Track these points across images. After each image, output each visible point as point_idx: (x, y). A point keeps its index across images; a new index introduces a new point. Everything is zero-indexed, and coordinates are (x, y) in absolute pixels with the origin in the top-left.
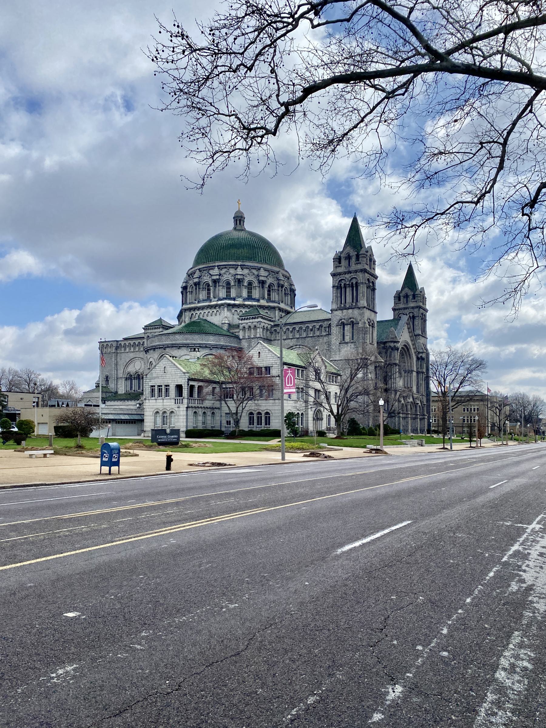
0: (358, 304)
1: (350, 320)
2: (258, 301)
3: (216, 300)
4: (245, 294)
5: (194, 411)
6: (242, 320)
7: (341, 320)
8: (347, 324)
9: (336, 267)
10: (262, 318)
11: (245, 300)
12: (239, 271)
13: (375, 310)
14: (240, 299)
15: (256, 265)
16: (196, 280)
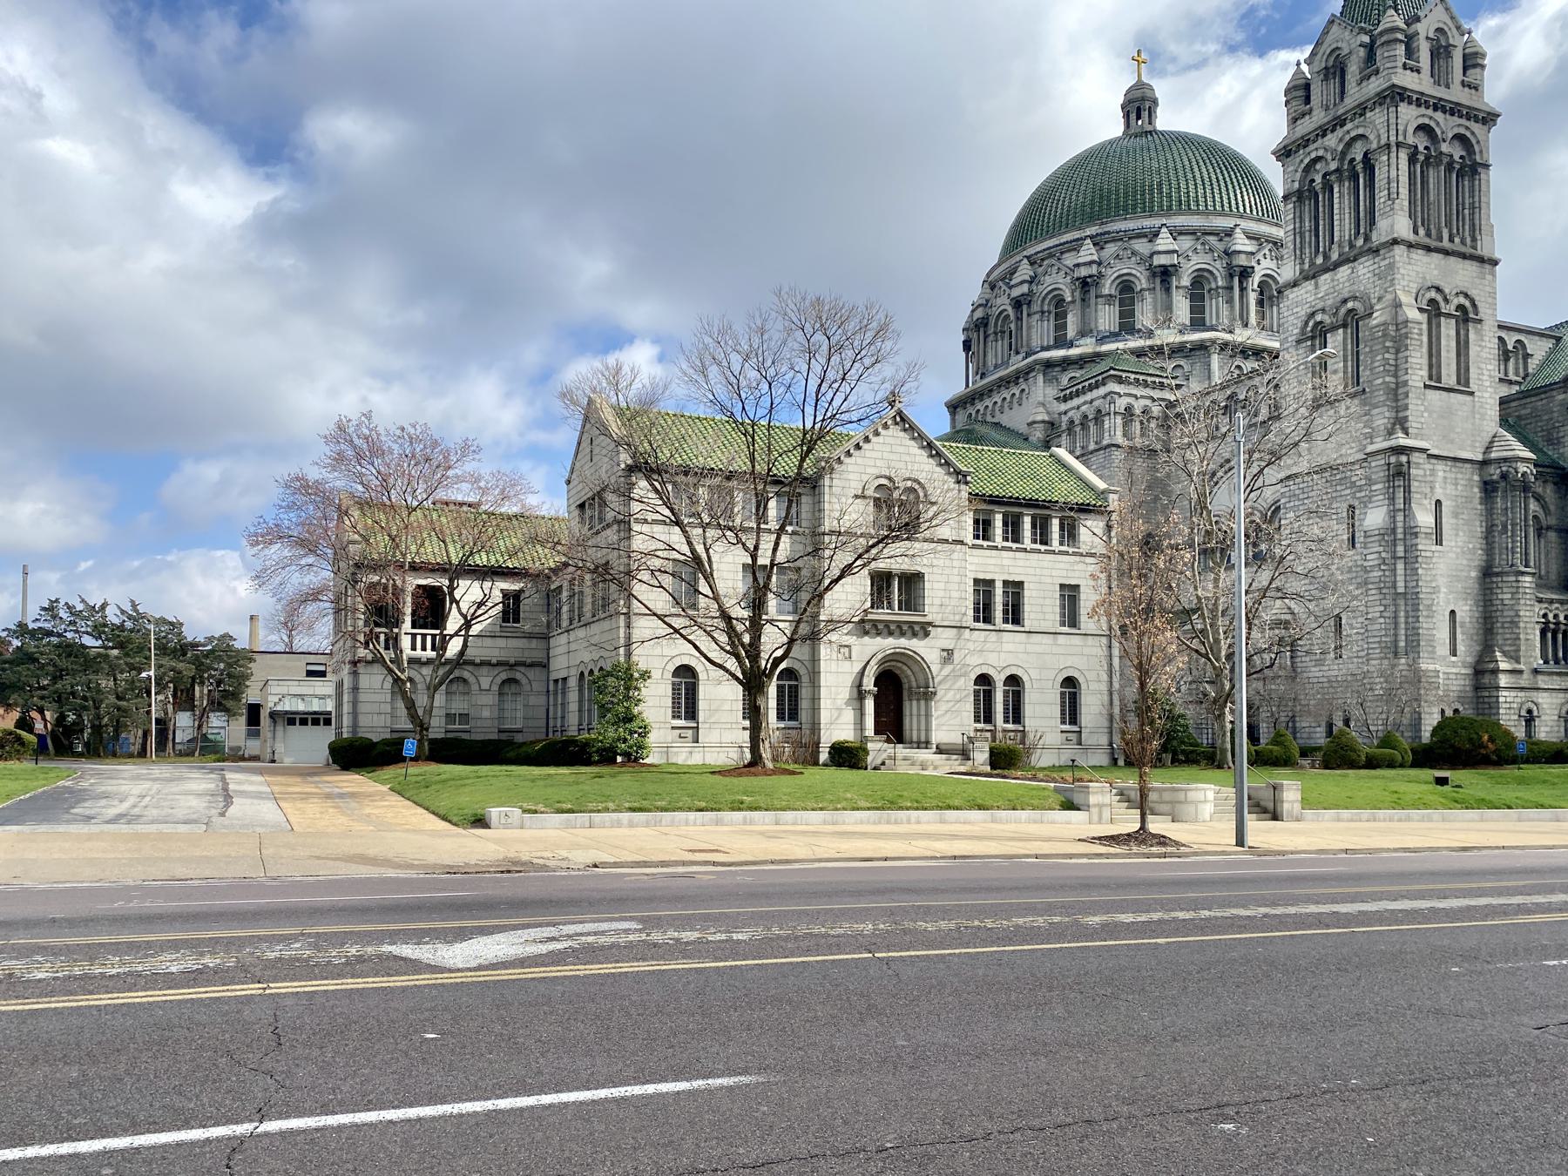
0: (1374, 237)
1: (1343, 311)
2: (1150, 334)
3: (1020, 357)
4: (1107, 318)
5: (504, 676)
6: (1065, 399)
7: (1313, 314)
8: (1334, 328)
9: (1294, 121)
10: (1120, 380)
11: (1102, 340)
12: (1088, 252)
13: (1483, 250)
14: (1088, 340)
15: (1147, 223)
16: (979, 314)
